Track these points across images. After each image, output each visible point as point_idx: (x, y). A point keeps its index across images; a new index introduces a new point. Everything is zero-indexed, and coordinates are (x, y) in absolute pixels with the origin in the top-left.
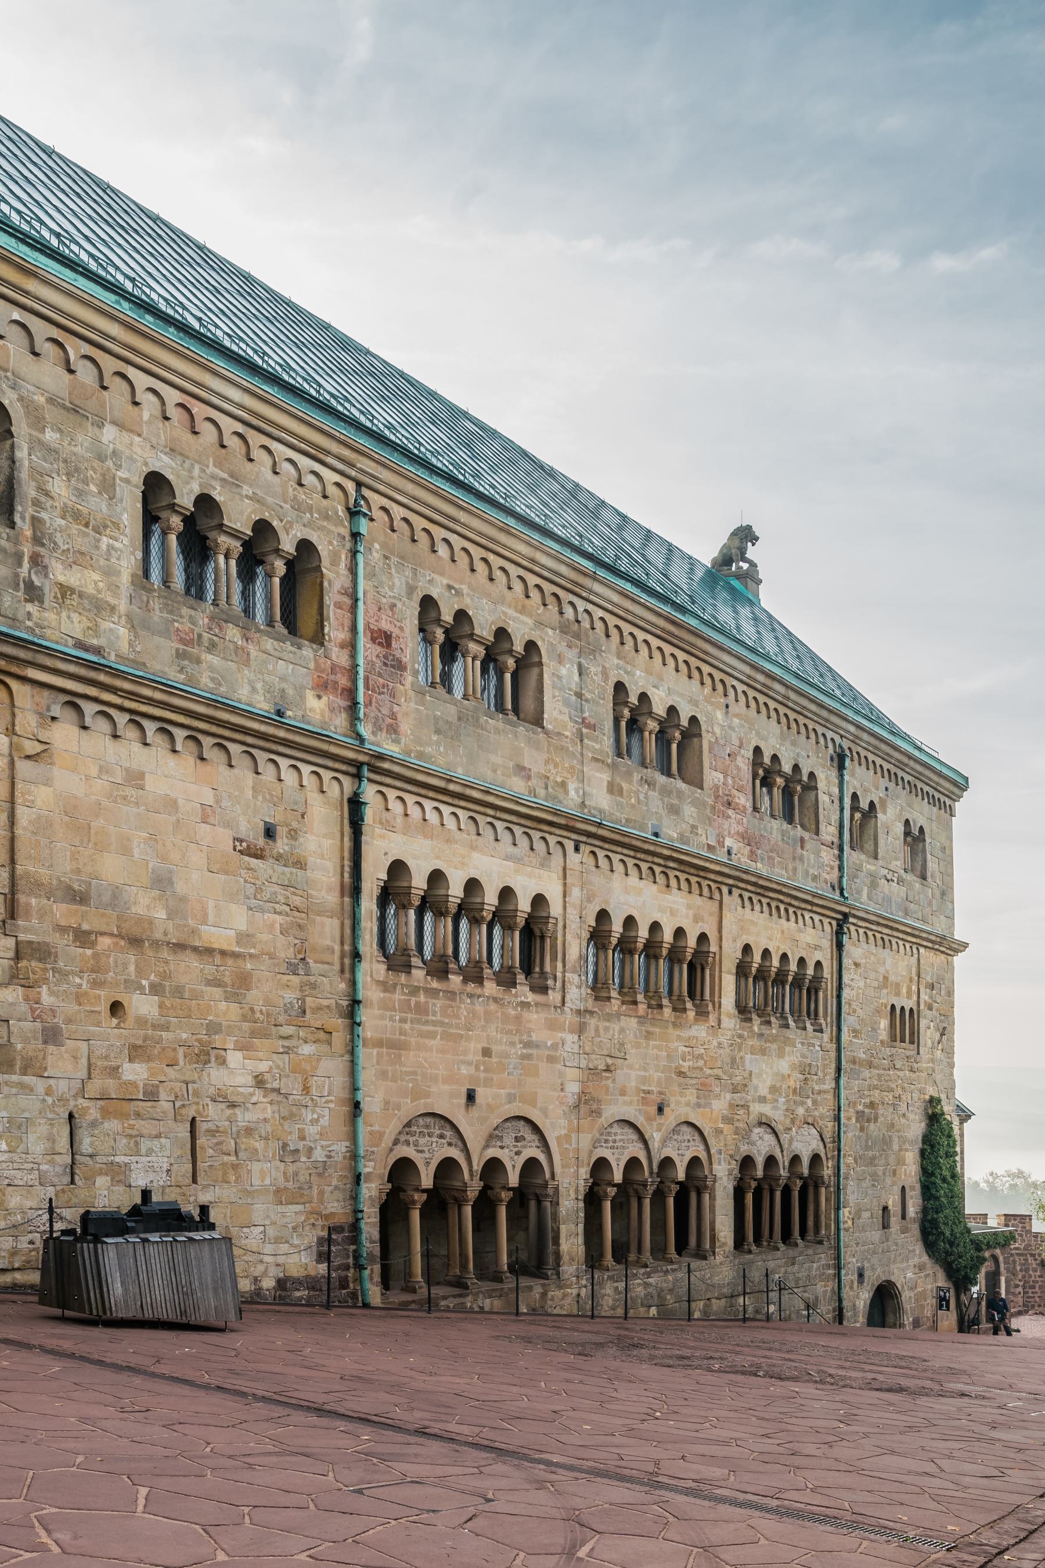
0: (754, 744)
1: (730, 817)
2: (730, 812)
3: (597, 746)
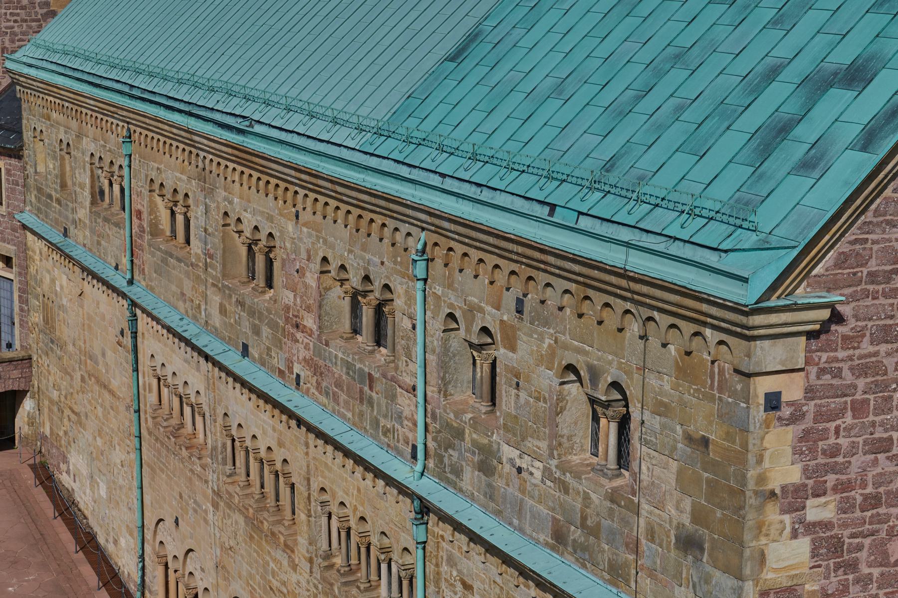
0: (321, 255)
1: (297, 341)
2: (299, 335)
3: (214, 273)
